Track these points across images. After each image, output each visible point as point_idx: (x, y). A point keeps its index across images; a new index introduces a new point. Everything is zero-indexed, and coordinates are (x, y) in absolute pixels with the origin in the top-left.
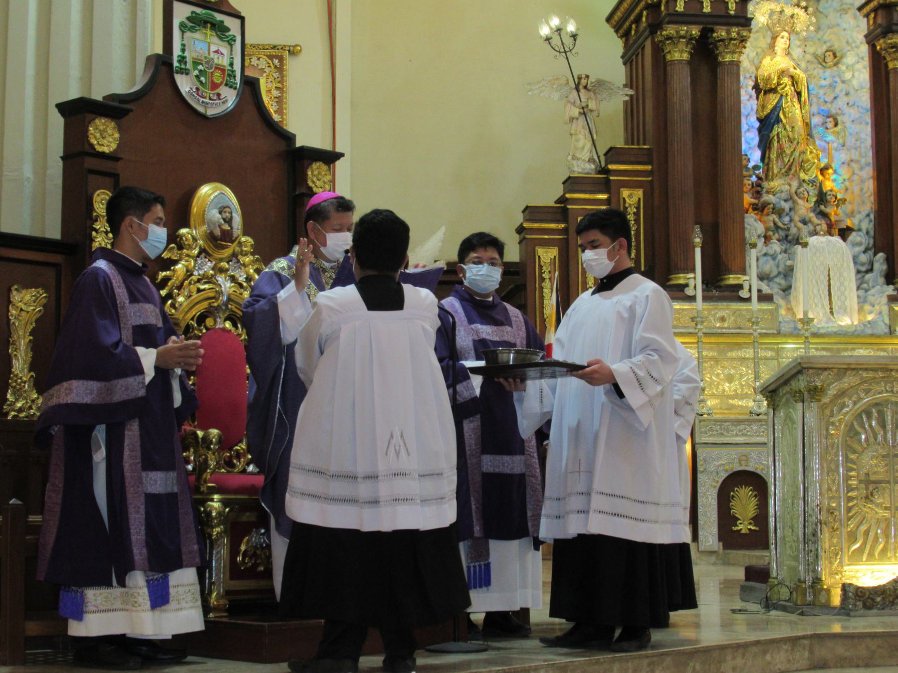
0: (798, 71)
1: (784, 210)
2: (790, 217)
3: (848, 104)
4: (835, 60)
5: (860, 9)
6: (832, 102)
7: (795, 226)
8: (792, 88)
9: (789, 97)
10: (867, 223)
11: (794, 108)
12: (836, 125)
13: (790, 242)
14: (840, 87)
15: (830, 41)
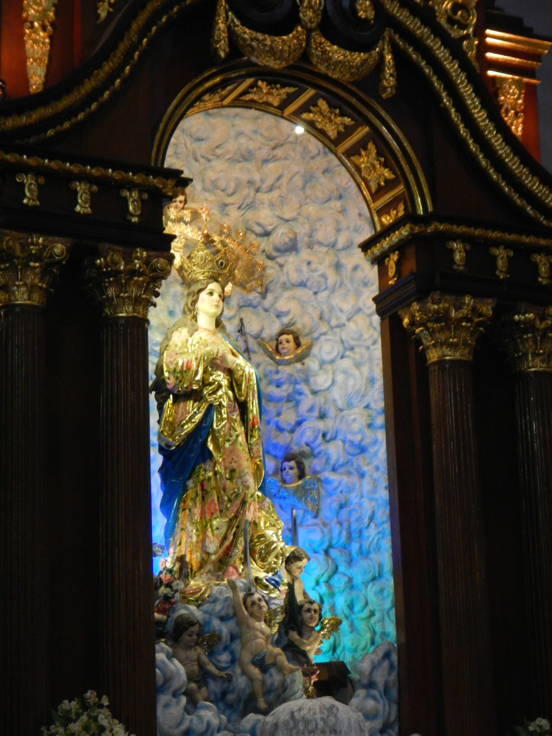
0: (240, 360)
1: (219, 638)
2: (232, 653)
3: (324, 435)
4: (299, 351)
5: (365, 246)
6: (292, 431)
7: (244, 673)
8: (230, 393)
9: (223, 411)
10: (386, 672)
11: (234, 434)
12: (301, 476)
13: (230, 706)
14: (307, 401)
15: (288, 312)
